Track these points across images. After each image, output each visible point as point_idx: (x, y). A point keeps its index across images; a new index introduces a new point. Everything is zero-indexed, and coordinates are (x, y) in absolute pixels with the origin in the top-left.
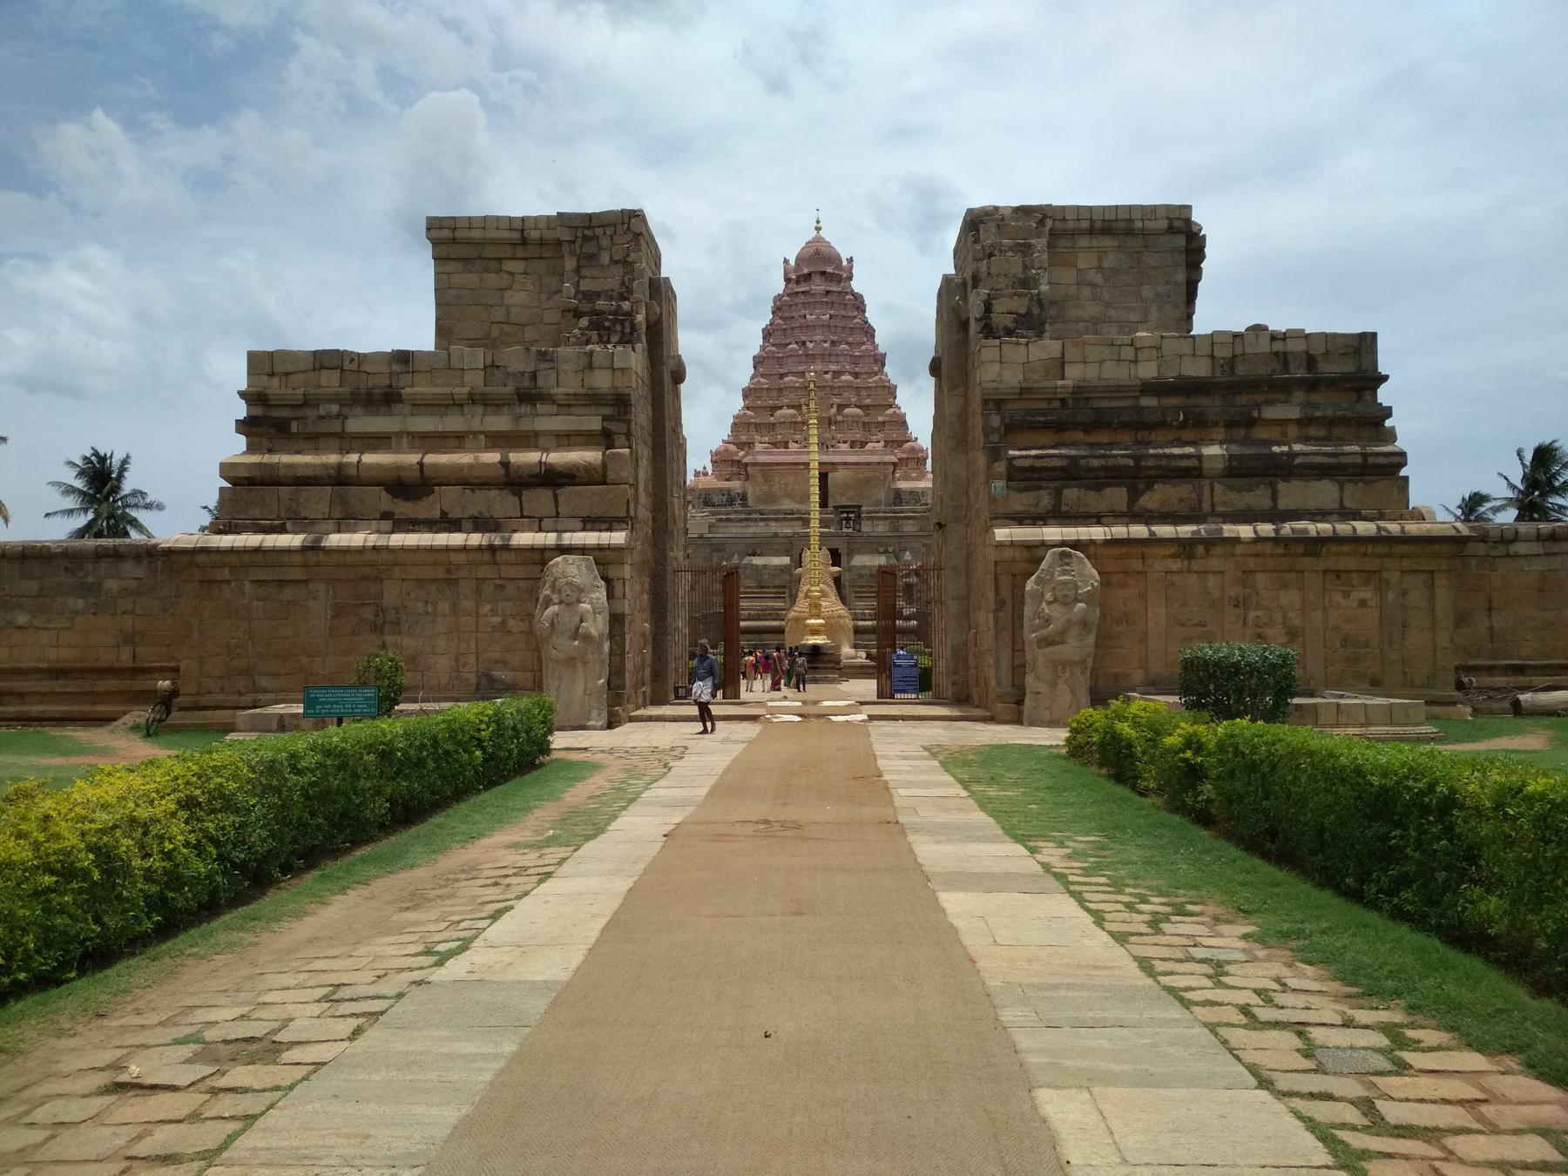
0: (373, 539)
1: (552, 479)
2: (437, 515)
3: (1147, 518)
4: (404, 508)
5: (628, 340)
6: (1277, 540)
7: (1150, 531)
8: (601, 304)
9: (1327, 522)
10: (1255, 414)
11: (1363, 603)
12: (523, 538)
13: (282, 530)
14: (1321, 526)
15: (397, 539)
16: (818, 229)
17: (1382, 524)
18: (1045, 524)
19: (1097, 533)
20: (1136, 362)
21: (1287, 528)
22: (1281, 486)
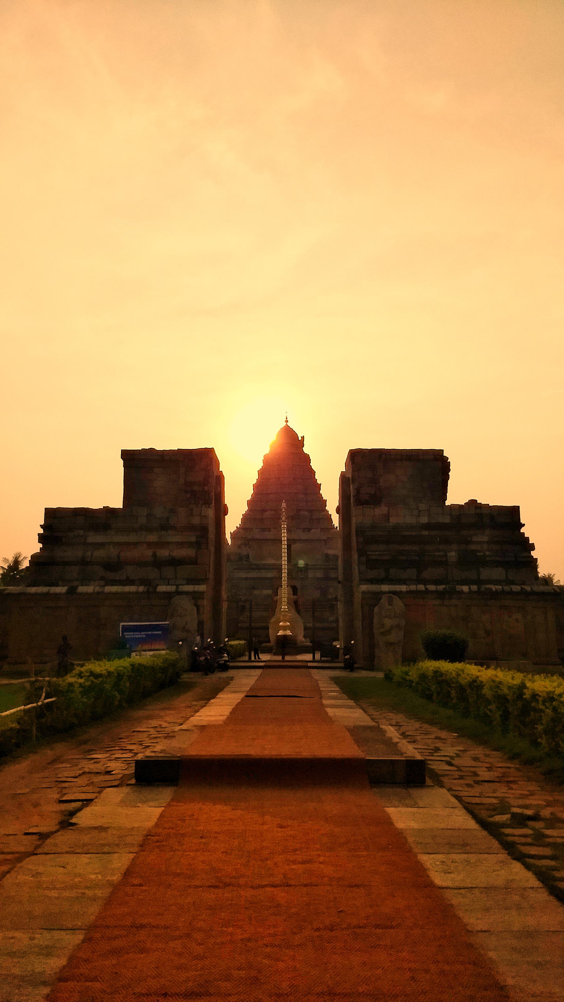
0: (97, 589)
1: (175, 562)
2: (125, 578)
3: (425, 582)
4: (111, 575)
5: (207, 503)
6: (478, 592)
7: (425, 587)
8: (196, 488)
9: (501, 585)
10: (469, 539)
11: (517, 620)
12: (162, 588)
13: (57, 585)
14: (497, 587)
15: (108, 589)
16: (287, 421)
17: (524, 587)
18: (383, 584)
19: (404, 588)
20: (419, 516)
21: (483, 587)
22: (481, 569)
